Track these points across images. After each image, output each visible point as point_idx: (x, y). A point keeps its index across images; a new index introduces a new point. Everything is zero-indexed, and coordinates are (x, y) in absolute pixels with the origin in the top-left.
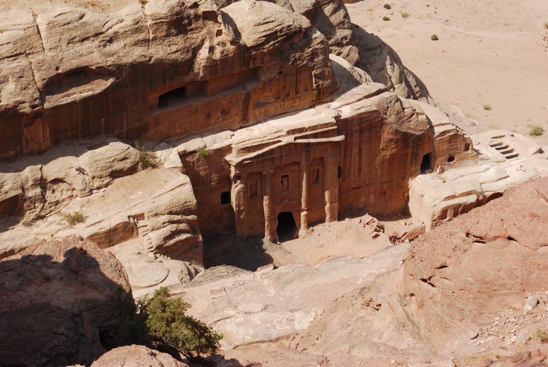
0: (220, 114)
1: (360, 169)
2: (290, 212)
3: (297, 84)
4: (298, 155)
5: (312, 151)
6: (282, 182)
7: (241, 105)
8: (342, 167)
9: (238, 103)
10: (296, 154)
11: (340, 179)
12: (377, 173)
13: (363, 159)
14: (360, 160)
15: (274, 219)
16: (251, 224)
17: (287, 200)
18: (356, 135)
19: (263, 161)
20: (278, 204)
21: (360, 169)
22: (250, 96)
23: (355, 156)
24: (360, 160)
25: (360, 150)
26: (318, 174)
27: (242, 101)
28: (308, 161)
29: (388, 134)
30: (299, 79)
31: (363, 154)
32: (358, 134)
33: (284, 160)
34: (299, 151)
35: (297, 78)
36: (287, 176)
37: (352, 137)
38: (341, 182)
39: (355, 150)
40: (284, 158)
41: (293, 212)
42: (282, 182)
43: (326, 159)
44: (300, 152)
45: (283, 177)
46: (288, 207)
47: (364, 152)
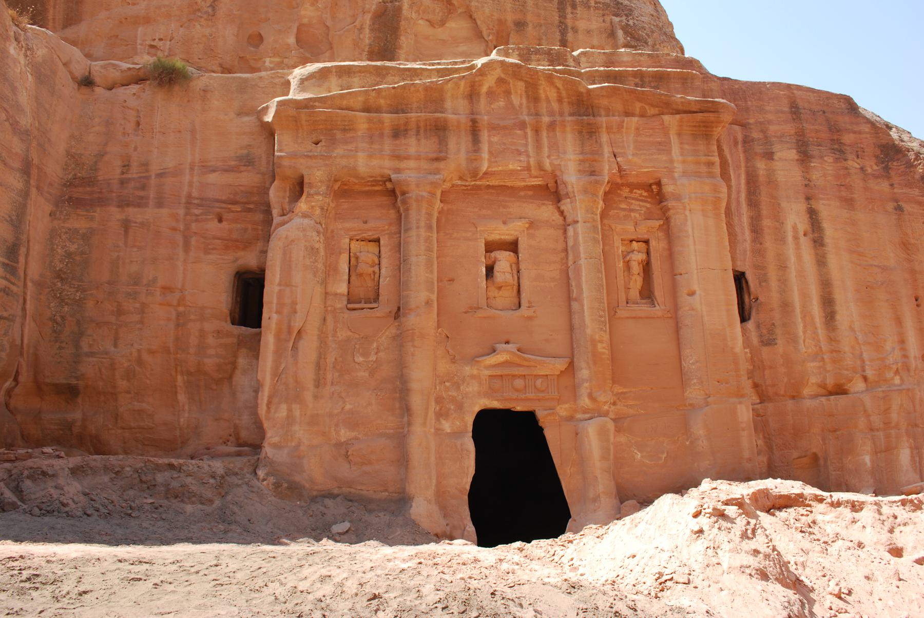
0: (292, 40)
1: (828, 302)
2: (530, 417)
3: (563, 33)
4: (545, 141)
5: (604, 138)
6: (490, 270)
7: (367, 31)
8: (750, 276)
9: (357, 23)
10: (537, 131)
11: (750, 325)
12: (902, 341)
13: (832, 261)
14: (821, 262)
15: (457, 434)
16: (345, 434)
17: (511, 347)
18: (786, 154)
19: (397, 133)
20: (474, 359)
21: (828, 302)
22: (399, 9)
23: (796, 238)
24: (821, 262)
25: (812, 214)
26: (647, 267)
27: (368, 18)
28: (593, 173)
29: (910, 185)
30: (569, 22)
31: (828, 240)
32: (793, 154)
33: (485, 147)
34: (546, 119)
35: (563, 16)
36: (513, 247)
37: (769, 156)
38: (755, 340)
39: (795, 217)
40: (484, 136)
41: (540, 414)
42: (490, 270)
43: (669, 189)
44: (552, 126)
45: (491, 247)
46: (519, 383)
47: (830, 232)
